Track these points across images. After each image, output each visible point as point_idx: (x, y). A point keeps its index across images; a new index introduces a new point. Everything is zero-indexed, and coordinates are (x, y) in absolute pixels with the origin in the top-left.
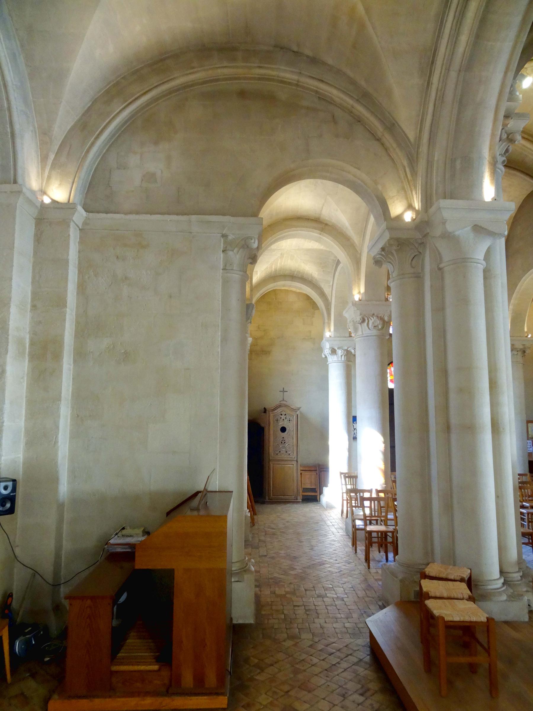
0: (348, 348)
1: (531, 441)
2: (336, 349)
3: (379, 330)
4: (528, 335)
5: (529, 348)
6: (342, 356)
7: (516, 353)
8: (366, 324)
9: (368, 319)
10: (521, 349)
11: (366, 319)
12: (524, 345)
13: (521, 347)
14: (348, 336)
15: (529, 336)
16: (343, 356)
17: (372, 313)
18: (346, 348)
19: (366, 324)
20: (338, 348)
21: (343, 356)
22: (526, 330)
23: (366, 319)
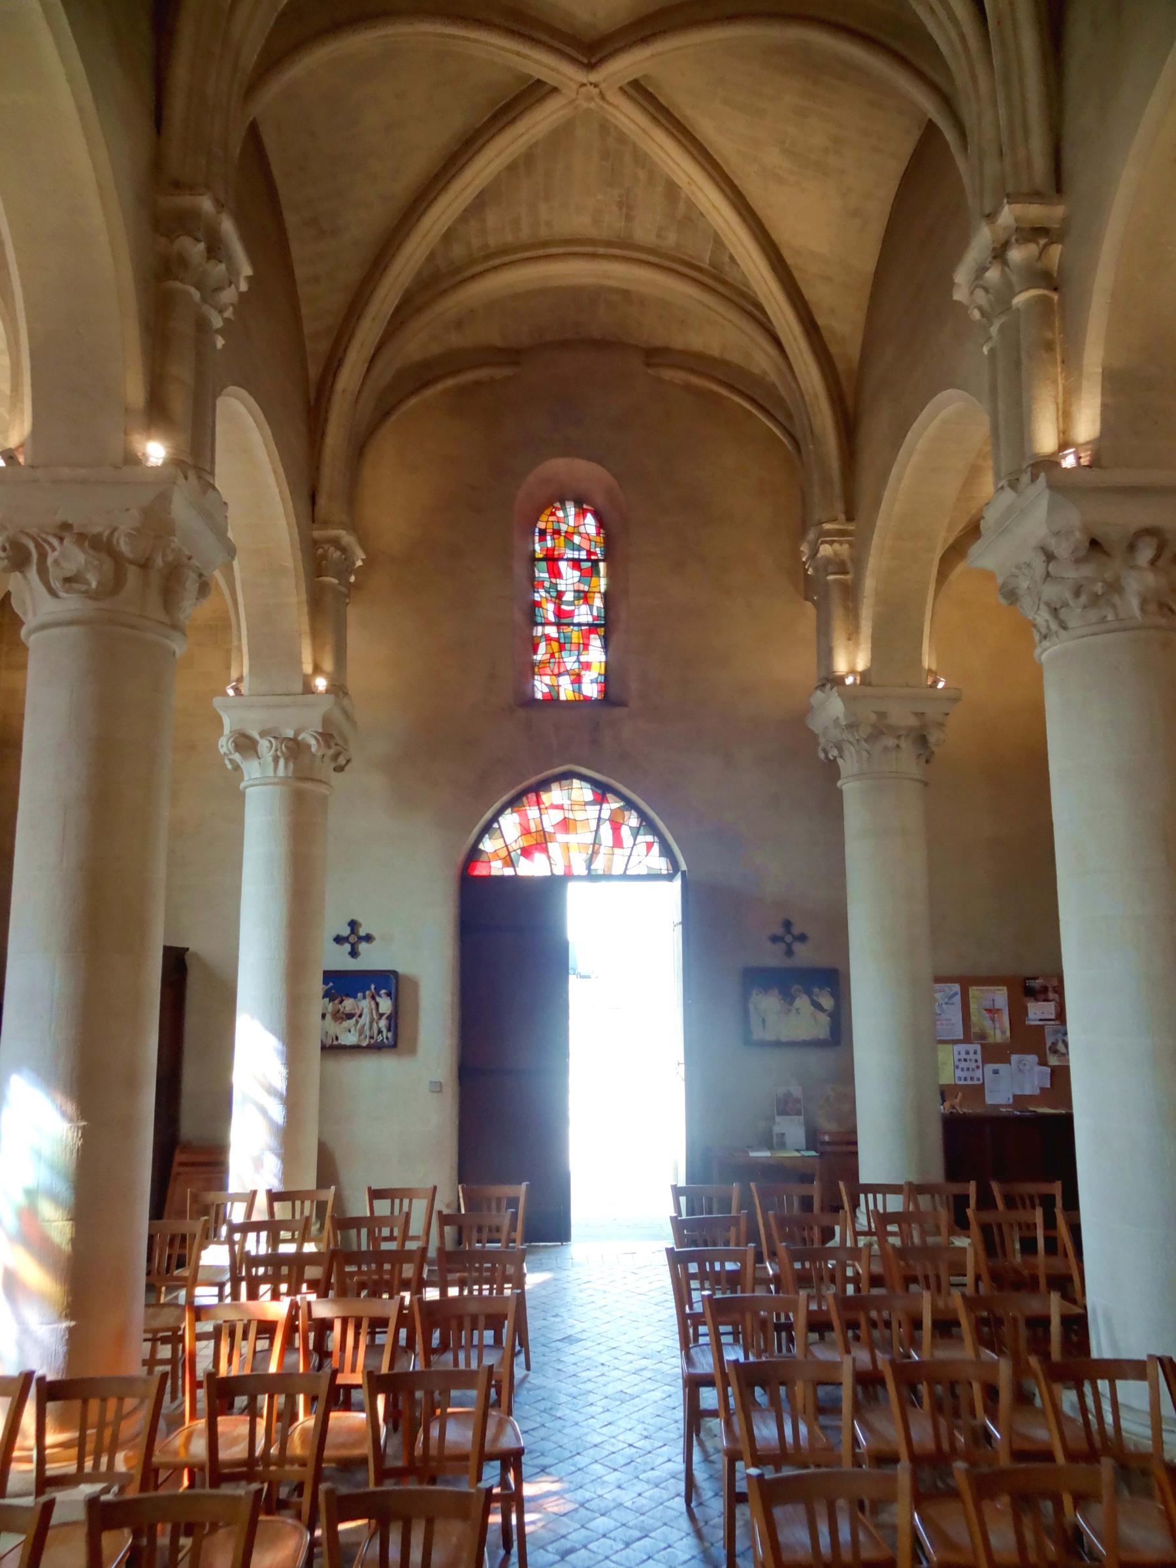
0: (297, 733)
1: (978, 1047)
2: (257, 737)
3: (89, 595)
4: (936, 682)
5: (941, 725)
6: (276, 760)
7: (890, 742)
8: (33, 573)
9: (38, 546)
10: (911, 729)
11: (31, 546)
12: (920, 715)
13: (913, 721)
14: (299, 687)
15: (941, 685)
16: (282, 762)
17: (60, 517)
18: (290, 733)
19: (33, 573)
20: (263, 734)
21: (282, 762)
22: (928, 661)
23: (31, 546)
